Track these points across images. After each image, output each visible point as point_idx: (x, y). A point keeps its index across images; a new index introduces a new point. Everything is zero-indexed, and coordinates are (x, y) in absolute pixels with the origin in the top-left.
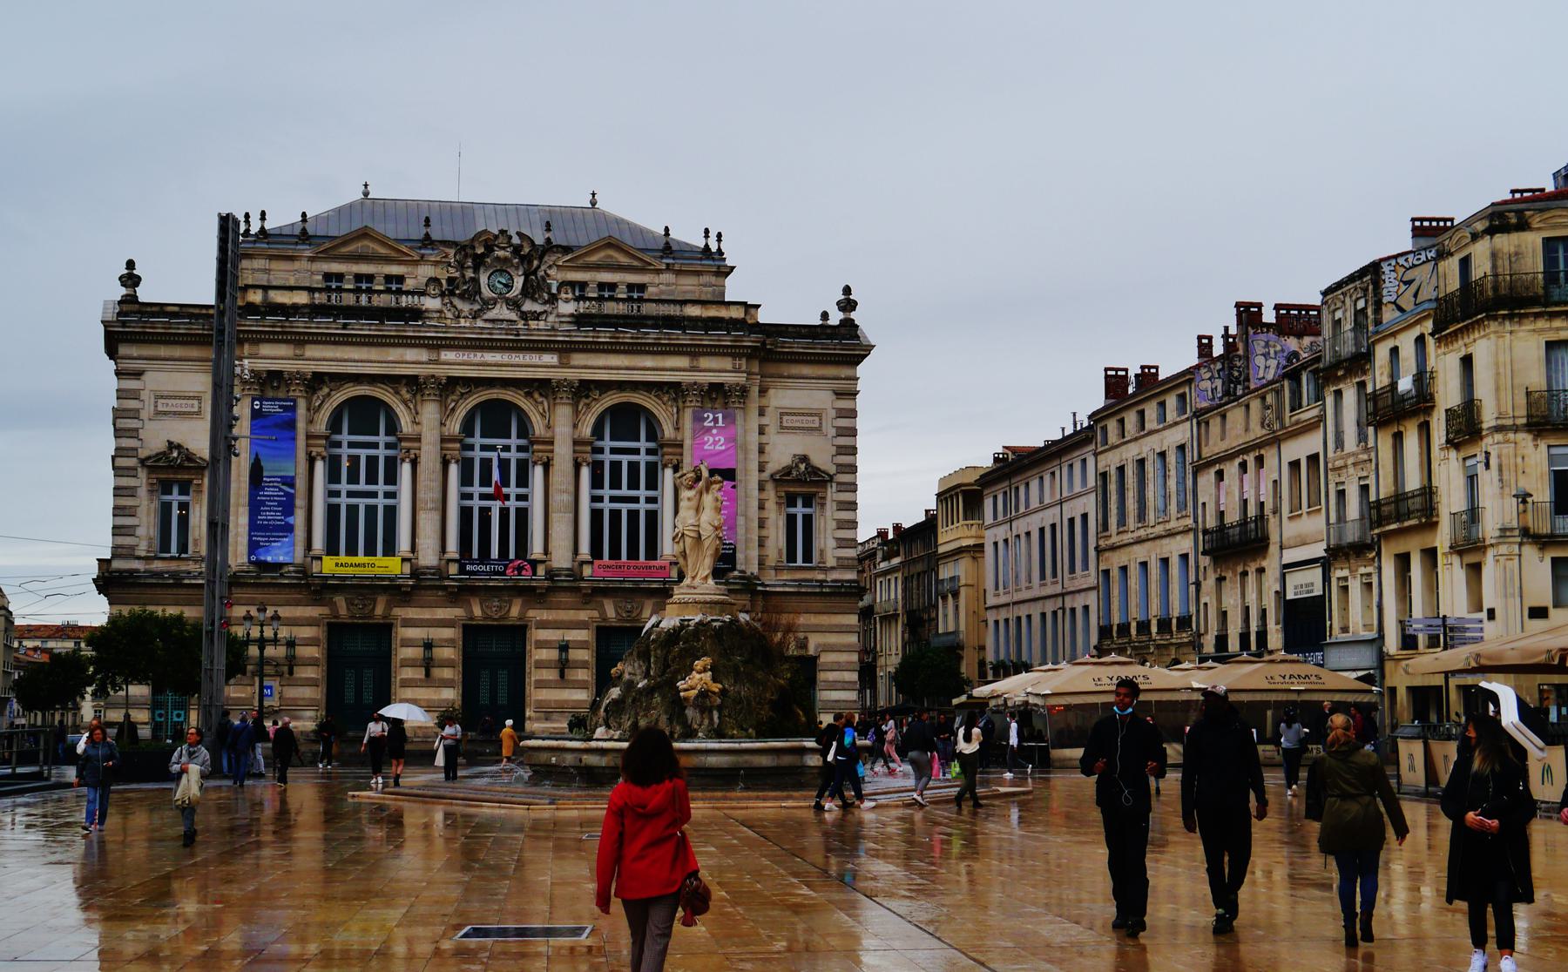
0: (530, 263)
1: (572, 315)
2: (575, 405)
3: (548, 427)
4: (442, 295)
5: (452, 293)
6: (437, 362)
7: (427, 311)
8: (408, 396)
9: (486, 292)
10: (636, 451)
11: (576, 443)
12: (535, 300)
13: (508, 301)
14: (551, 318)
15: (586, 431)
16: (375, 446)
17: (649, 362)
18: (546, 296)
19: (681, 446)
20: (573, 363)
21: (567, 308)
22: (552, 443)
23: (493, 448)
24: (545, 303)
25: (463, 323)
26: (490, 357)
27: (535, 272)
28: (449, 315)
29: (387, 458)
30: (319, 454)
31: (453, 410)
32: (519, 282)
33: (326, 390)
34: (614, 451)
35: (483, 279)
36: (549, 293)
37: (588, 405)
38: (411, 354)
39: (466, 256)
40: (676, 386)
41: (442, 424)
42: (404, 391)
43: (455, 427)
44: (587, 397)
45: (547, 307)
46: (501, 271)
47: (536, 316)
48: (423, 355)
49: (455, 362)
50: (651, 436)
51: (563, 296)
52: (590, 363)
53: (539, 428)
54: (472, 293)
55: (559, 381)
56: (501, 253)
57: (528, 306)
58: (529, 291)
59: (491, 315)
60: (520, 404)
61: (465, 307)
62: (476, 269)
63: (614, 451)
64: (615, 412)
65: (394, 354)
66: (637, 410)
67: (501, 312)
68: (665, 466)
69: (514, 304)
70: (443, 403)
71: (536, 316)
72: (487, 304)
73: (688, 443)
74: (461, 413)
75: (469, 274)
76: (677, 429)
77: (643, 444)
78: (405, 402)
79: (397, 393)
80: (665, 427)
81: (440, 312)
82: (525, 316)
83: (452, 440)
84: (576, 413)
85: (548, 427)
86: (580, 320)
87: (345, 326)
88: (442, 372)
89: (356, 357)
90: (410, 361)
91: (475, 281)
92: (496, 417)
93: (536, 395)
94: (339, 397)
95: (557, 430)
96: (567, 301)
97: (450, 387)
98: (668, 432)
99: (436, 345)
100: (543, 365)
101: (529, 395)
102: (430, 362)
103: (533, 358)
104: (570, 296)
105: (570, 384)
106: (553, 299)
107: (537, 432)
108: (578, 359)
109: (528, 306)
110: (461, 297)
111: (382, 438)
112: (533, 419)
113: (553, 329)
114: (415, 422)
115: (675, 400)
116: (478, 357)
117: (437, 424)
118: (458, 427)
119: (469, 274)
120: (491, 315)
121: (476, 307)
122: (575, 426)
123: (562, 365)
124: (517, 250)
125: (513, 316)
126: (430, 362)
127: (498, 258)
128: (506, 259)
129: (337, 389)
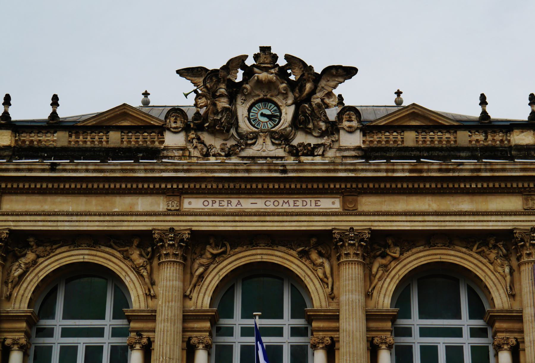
0: (302, 88)
1: (358, 148)
2: (367, 267)
3: (332, 297)
4: (187, 129)
5: (200, 128)
6: (178, 212)
7: (166, 149)
8: (140, 261)
9: (245, 126)
10: (457, 332)
11: (370, 317)
12: (309, 132)
13: (272, 135)
14: (331, 154)
15: (384, 301)
16: (99, 332)
17: (465, 204)
18: (323, 125)
19: (519, 319)
20: (361, 208)
21: (353, 140)
22: (336, 318)
23: (259, 333)
24: (322, 135)
25: (212, 160)
26: (248, 204)
27: (308, 99)
28: (196, 153)
29: (114, 349)
30: (15, 342)
31: (201, 277)
32: (288, 113)
33: (31, 256)
34: (425, 332)
35: (242, 111)
36: (327, 121)
37: (385, 267)
38: (143, 203)
39: (218, 82)
40: (505, 236)
41: (186, 297)
42: (135, 254)
43: (203, 299)
44: (384, 256)
45: (325, 140)
46: (265, 101)
47: (310, 151)
48: (160, 204)
49: (202, 212)
50: (477, 311)
51: (346, 124)
52: (385, 208)
53: (318, 299)
54: (225, 125)
55: (343, 233)
56: (263, 76)
57: (300, 139)
58: (298, 123)
59: (249, 152)
60: (293, 268)
61: (215, 143)
62: (232, 100)
63: (425, 332)
64: (421, 276)
65: (121, 203)
66: (456, 275)
67: (265, 148)
68: (498, 348)
69: (282, 139)
70: (186, 266)
71: (310, 151)
72: (247, 139)
73: (528, 313)
74: (213, 280)
75: (223, 103)
76: (512, 296)
77: (466, 322)
78: (136, 270)
79: (127, 257)
80: (495, 294)
81: (183, 149)
82: (295, 152)
83: (198, 316)
84: (369, 277)
85: (332, 297)
86: (367, 153)
87: (53, 168)
88: (182, 224)
89: (70, 208)
90: (143, 212)
91: (233, 115)
92: (262, 287)
93: (314, 256)
94: (49, 265)
95: (343, 298)
96: (351, 131)
97: (196, 245)
98: (500, 300)
99: (177, 188)
100: (322, 212)
101: (304, 255)
102: (168, 213)
103: (308, 204)
104: (355, 124)
105: (358, 235)
106: (333, 129)
107: (317, 305)
108: (368, 203)
109: (300, 139)
110: (213, 131)
111: (108, 322)
112: (311, 287)
113: (333, 163)
114: (150, 296)
115: (506, 257)
116: (234, 204)
117: (178, 295)
118: (207, 300)
119: (223, 103)
120: (249, 152)
121: (231, 143)
122: (368, 295)
123: (347, 211)
124: (282, 73)
125: (280, 152)
126: (168, 213)
127: (259, 81)
128: (269, 85)
129: (47, 255)
